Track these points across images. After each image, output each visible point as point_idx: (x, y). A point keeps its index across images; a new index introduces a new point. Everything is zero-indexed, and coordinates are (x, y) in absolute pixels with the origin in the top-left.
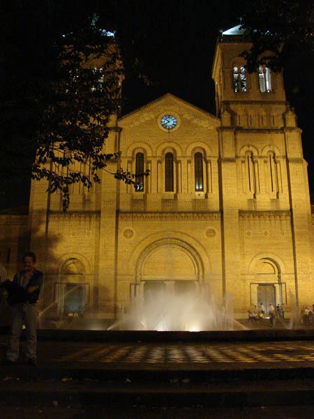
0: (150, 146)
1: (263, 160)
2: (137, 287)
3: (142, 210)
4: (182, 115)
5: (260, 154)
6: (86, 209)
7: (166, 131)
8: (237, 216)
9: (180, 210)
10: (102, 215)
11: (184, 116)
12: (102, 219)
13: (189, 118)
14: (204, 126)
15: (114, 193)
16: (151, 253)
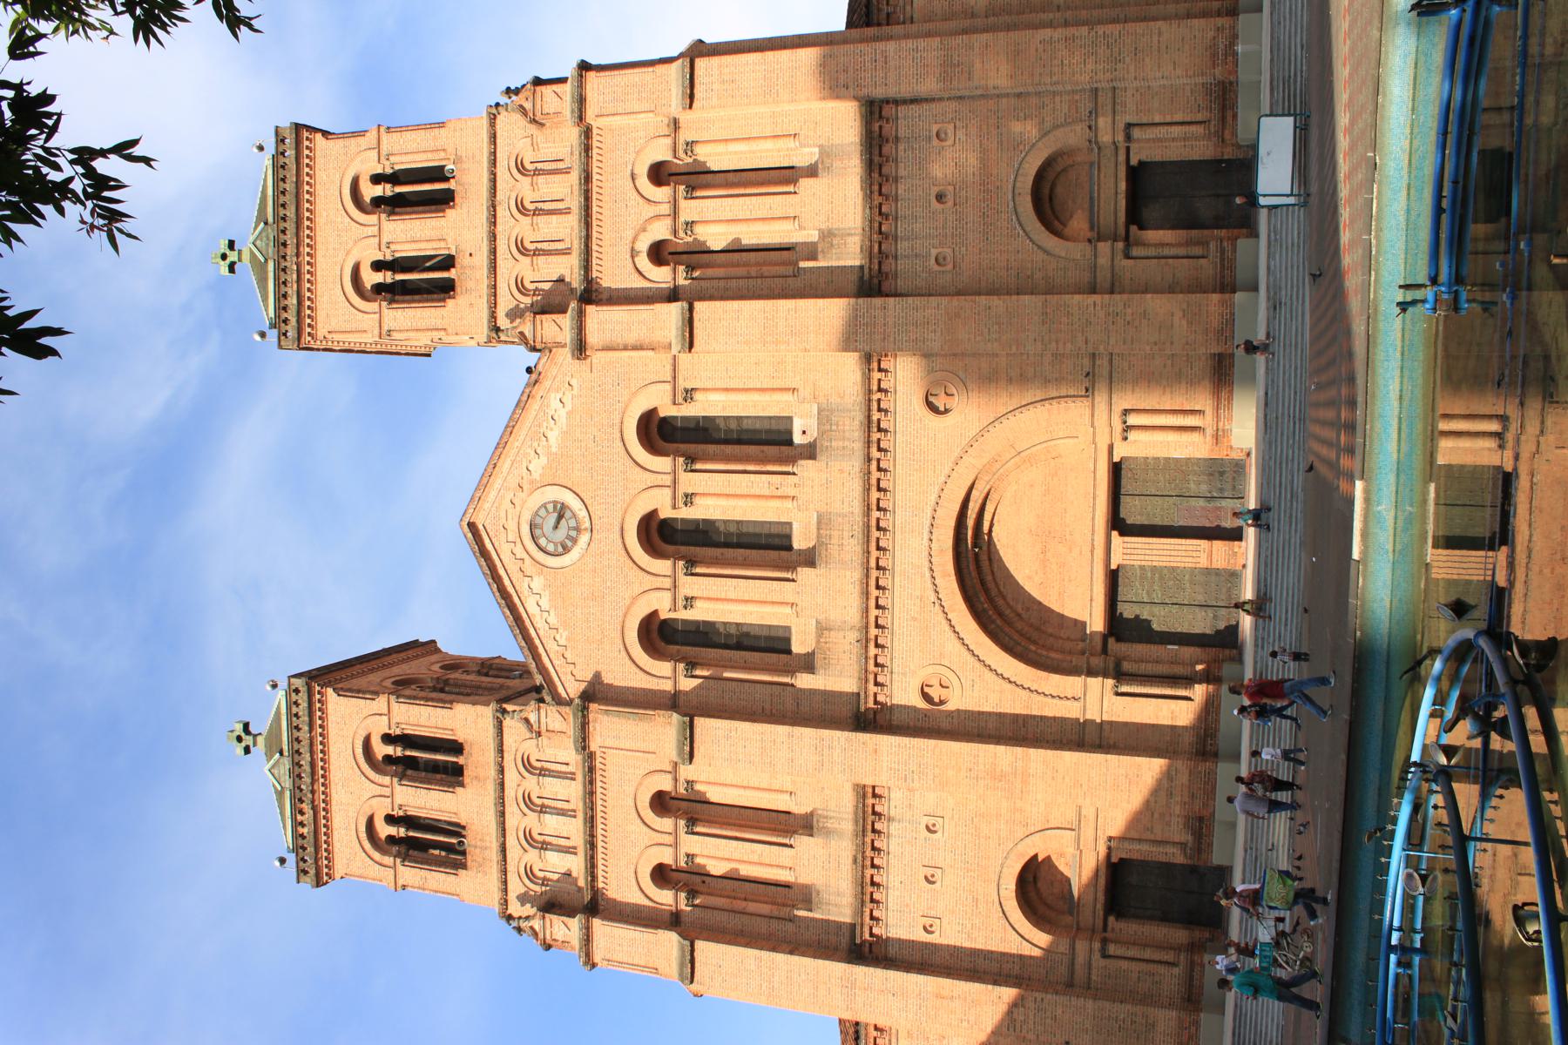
0: (635, 599)
1: (683, 204)
2: (1126, 666)
3: (853, 636)
4: (532, 482)
5: (665, 209)
6: (848, 826)
7: (584, 539)
8: (878, 301)
9: (857, 507)
10: (869, 782)
11: (536, 475)
12: (881, 780)
13: (544, 460)
14: (569, 407)
15: (790, 736)
16: (1008, 612)
